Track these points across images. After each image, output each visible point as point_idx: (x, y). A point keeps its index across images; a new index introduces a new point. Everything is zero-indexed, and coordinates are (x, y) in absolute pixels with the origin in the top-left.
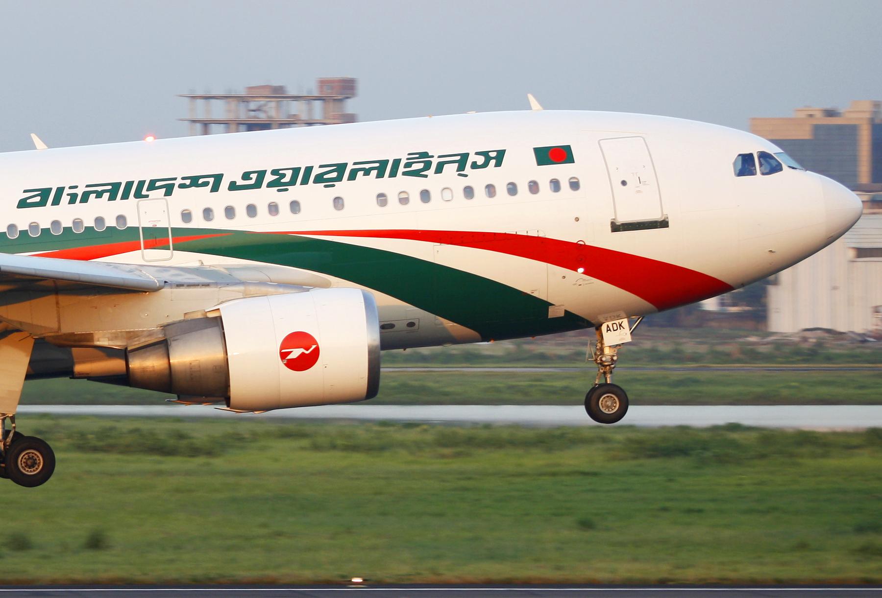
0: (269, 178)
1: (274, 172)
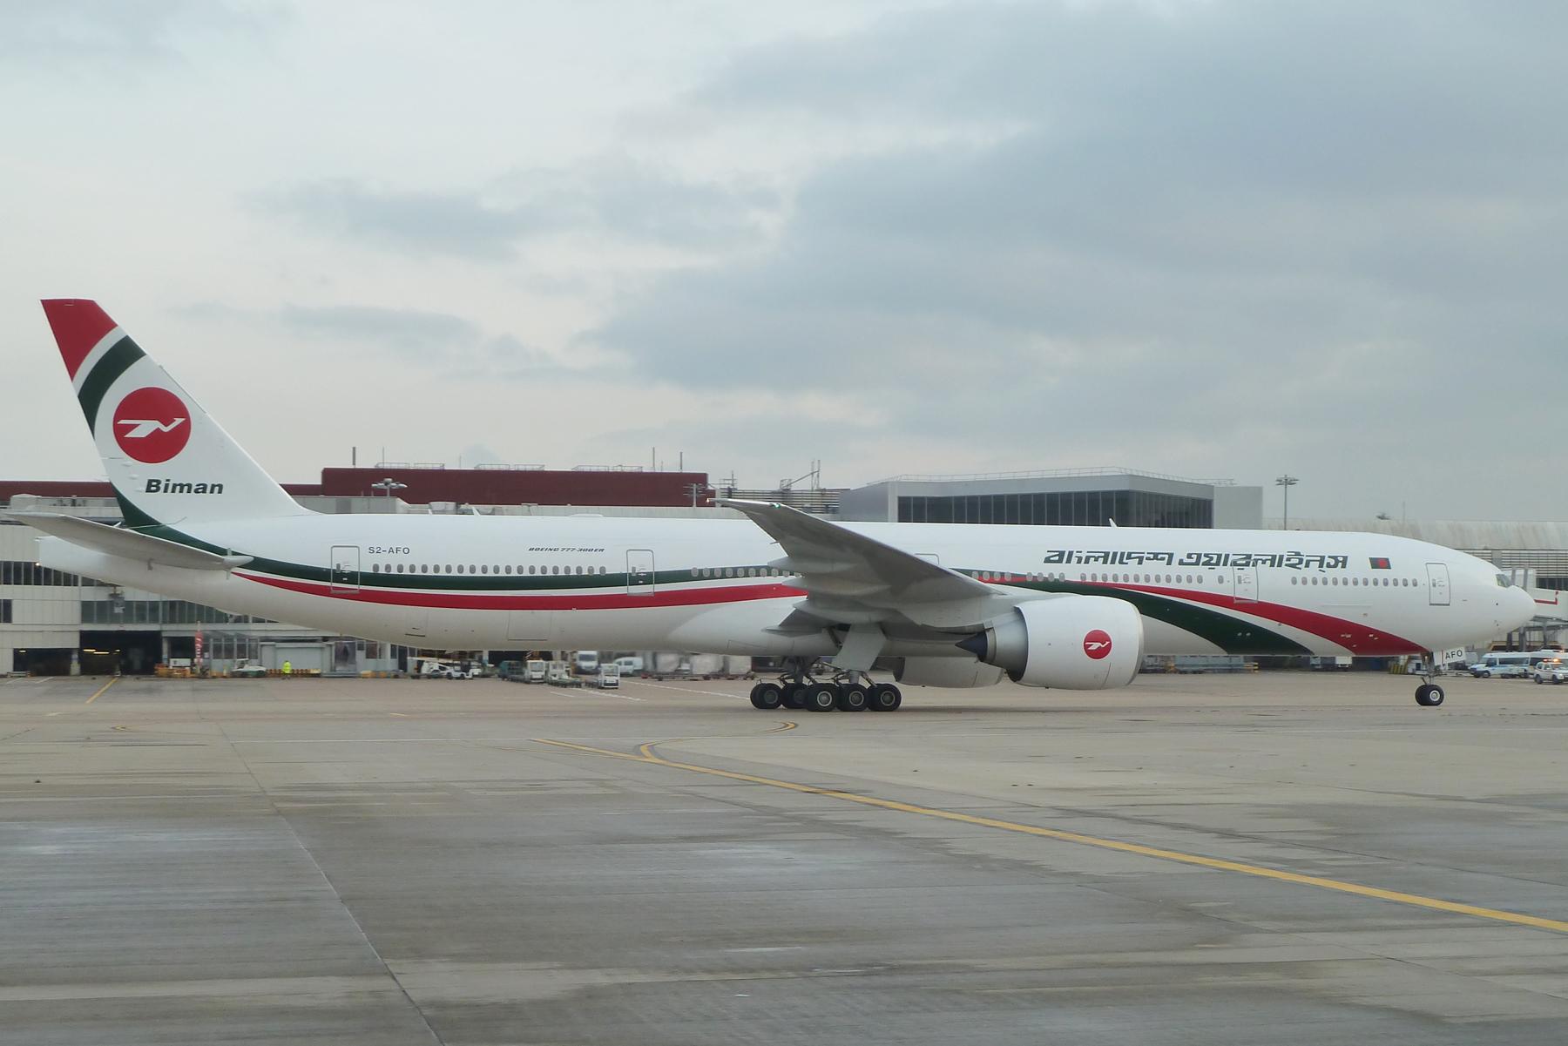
0: (1204, 559)
1: (1206, 555)
